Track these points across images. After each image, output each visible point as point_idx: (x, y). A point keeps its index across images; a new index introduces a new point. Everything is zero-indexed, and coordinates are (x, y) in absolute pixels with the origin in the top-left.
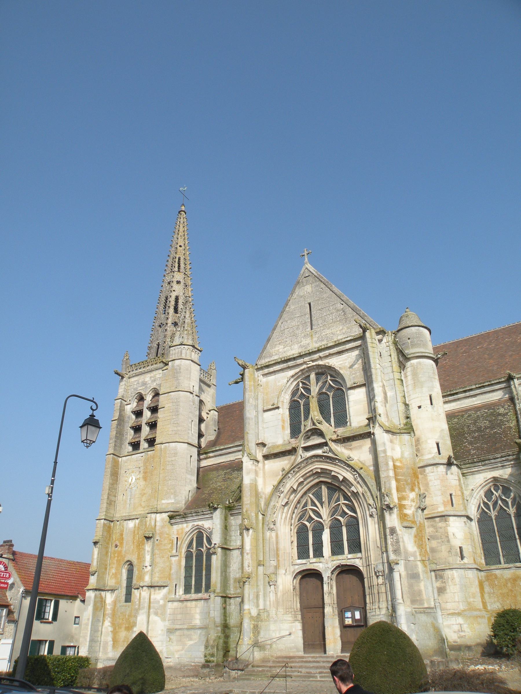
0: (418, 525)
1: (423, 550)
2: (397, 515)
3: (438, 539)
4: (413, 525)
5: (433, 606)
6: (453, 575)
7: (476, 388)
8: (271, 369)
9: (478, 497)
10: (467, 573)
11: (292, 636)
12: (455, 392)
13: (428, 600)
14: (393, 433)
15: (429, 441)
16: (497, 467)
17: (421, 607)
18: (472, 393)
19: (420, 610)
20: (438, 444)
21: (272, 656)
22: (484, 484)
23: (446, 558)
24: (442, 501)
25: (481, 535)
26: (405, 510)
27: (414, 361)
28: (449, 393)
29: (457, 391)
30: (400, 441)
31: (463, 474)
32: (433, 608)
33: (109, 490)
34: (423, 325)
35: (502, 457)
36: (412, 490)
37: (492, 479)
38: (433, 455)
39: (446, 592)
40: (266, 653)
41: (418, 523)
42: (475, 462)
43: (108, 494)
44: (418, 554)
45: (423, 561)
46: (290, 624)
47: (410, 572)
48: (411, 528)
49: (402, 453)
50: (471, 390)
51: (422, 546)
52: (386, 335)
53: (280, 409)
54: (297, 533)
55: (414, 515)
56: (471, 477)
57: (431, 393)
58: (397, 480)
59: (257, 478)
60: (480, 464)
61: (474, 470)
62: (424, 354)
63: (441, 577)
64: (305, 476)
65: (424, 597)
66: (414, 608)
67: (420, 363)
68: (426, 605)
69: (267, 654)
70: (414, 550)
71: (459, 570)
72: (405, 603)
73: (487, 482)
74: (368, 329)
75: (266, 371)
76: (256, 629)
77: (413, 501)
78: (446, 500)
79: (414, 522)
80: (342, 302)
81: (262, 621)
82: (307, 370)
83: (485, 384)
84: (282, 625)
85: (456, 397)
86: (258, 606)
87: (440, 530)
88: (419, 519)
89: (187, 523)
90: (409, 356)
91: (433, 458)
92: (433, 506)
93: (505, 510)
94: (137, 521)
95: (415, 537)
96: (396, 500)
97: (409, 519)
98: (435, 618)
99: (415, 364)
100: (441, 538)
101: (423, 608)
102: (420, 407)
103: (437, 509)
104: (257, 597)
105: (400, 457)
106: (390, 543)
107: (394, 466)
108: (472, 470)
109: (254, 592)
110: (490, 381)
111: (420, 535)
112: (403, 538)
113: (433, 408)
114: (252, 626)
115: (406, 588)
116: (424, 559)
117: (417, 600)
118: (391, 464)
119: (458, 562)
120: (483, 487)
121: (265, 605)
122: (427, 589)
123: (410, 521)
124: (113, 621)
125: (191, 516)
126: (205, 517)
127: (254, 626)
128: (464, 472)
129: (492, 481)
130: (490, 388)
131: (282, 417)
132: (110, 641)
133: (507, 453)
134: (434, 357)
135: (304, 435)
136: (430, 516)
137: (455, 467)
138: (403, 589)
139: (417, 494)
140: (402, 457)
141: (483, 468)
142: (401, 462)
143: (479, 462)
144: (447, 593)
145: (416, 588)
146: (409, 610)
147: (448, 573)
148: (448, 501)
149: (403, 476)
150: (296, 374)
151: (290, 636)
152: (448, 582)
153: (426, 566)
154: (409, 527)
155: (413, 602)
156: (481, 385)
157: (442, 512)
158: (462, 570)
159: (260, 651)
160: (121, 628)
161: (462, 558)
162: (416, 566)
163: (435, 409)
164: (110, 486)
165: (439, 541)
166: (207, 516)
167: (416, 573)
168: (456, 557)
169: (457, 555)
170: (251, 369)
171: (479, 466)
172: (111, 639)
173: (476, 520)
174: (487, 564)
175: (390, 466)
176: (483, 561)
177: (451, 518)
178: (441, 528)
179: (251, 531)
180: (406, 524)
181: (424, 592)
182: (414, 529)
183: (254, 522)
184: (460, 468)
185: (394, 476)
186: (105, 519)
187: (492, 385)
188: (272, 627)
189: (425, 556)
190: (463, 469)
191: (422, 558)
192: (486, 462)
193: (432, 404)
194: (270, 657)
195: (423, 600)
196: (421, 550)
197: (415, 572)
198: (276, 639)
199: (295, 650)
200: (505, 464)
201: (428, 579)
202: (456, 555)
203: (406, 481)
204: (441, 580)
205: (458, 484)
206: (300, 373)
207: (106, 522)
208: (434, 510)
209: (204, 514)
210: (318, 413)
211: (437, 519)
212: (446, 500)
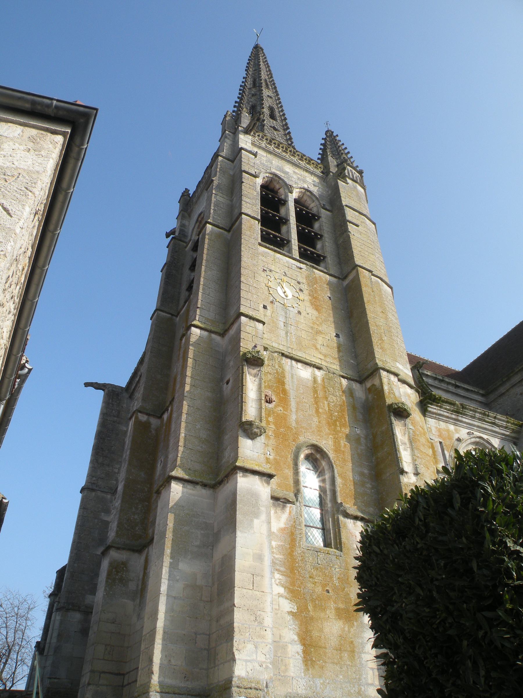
89: (455, 424)
94: (319, 374)
124: (293, 584)
125: (471, 417)
126: (494, 429)
132: (292, 642)
160: (323, 609)
166: (497, 429)
172: (296, 638)
209: (494, 424)
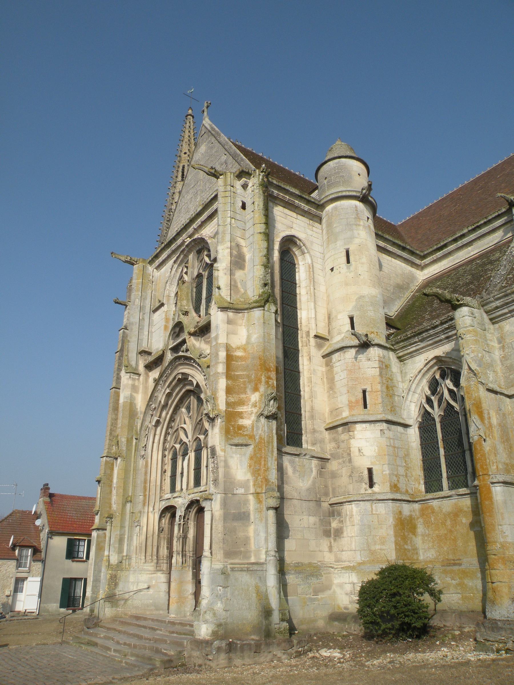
0: (257, 441)
1: (259, 478)
2: (221, 428)
3: (339, 459)
4: (250, 442)
5: (262, 561)
6: (351, 511)
7: (469, 231)
8: (161, 259)
9: (419, 391)
10: (376, 507)
11: (151, 591)
12: (442, 244)
13: (257, 552)
14: (238, 310)
15: (340, 316)
16: (441, 340)
17: (246, 561)
18: (466, 240)
19: (243, 566)
20: (352, 319)
21: (126, 614)
22: (425, 369)
23: (346, 486)
24: (347, 402)
25: (422, 448)
26: (241, 420)
27: (329, 208)
28: (435, 247)
29: (445, 242)
30: (248, 320)
31: (401, 359)
32: (262, 564)
33: (112, 425)
34: (349, 153)
35: (442, 324)
36: (256, 389)
37: (435, 361)
38: (343, 335)
39: (342, 536)
40: (118, 609)
41: (257, 437)
42: (410, 338)
43: (111, 430)
44: (251, 484)
45: (257, 494)
46: (150, 576)
47: (232, 511)
48: (246, 445)
49: (249, 337)
50: (463, 236)
51: (259, 472)
52: (252, 176)
53: (166, 306)
54: (171, 459)
55: (253, 427)
56: (409, 361)
57: (347, 247)
58: (229, 376)
59: (135, 394)
60: (417, 340)
61: (412, 350)
62: (340, 194)
63: (339, 514)
64: (172, 386)
65: (253, 546)
66: (232, 564)
67: (335, 208)
68: (253, 560)
69: (120, 612)
70: (247, 478)
71: (361, 503)
72: (214, 556)
73: (428, 366)
74: (221, 175)
75: (157, 262)
76: (114, 581)
77: (255, 405)
78: (353, 400)
79: (252, 437)
80: (226, 153)
81: (122, 570)
82: (187, 249)
83: (480, 223)
84: (140, 576)
85: (445, 251)
86: (120, 551)
87: (342, 445)
88: (260, 432)
90: (322, 202)
91: (343, 339)
92: (337, 411)
93: (453, 407)
95: (251, 458)
96: (222, 406)
97: (245, 433)
98: (263, 579)
99: (330, 211)
100: (343, 457)
101: (248, 564)
102: (332, 270)
103: (341, 414)
104: (121, 541)
105: (244, 342)
106: (211, 469)
107: (230, 358)
108: (409, 351)
109: (117, 535)
110: (486, 218)
111: (258, 455)
112: (226, 461)
113: (348, 268)
114: (108, 576)
115: (220, 535)
116: (260, 492)
117: (241, 552)
118: (222, 354)
119: (362, 491)
120: (424, 375)
121: (128, 550)
122: (258, 535)
123: (246, 435)
127: (111, 577)
128: (401, 354)
129: (435, 364)
130: (488, 227)
131: (166, 315)
133: (448, 316)
134: (358, 194)
135: (172, 333)
136: (331, 426)
137: (376, 348)
138: (213, 535)
139: (261, 395)
140: (248, 342)
141: (422, 345)
142: (245, 350)
143: (414, 336)
144: (343, 537)
145: (241, 534)
146: (218, 566)
147: (347, 507)
148: (357, 402)
149: (245, 370)
150: (178, 258)
151: (147, 590)
152: (345, 522)
153: (260, 502)
154: (242, 445)
155: (228, 554)
156: (475, 226)
157: (346, 418)
158: (368, 504)
159: (112, 607)
161: (371, 484)
162: (246, 502)
163: (352, 268)
164: (113, 422)
165: (340, 461)
167: (244, 513)
168: (359, 484)
169: (361, 480)
170: (141, 264)
171: (416, 342)
173: (417, 425)
174: (427, 492)
175: (220, 358)
176: (422, 488)
177: (358, 426)
178: (343, 442)
179: (119, 460)
180: (236, 441)
181: (252, 541)
182: (251, 448)
183: (124, 448)
184: (394, 350)
185: (225, 371)
186: (107, 457)
187: (489, 222)
188: (132, 578)
189: (261, 487)
190: (397, 350)
191: (256, 490)
192: (424, 334)
193: (348, 261)
194: (123, 615)
195: (250, 552)
196: (257, 478)
197: (243, 510)
198: (134, 592)
199: (153, 608)
200: (450, 334)
201: (261, 520)
202: (361, 480)
203: (248, 376)
204: (338, 518)
205: (378, 373)
206: (182, 256)
207: (108, 459)
208: (337, 416)
210: (188, 302)
211: (340, 429)
212: (353, 400)
